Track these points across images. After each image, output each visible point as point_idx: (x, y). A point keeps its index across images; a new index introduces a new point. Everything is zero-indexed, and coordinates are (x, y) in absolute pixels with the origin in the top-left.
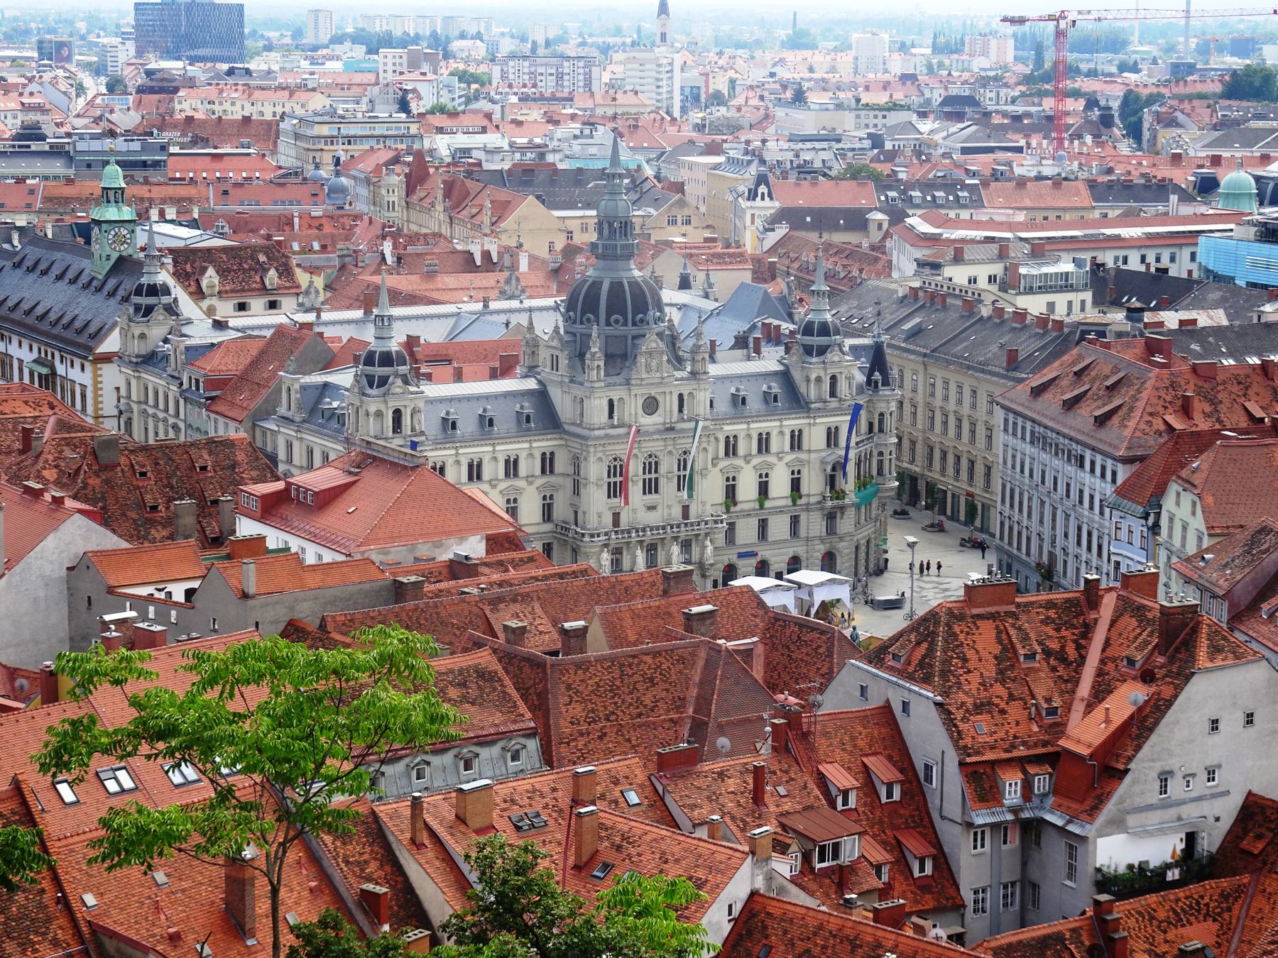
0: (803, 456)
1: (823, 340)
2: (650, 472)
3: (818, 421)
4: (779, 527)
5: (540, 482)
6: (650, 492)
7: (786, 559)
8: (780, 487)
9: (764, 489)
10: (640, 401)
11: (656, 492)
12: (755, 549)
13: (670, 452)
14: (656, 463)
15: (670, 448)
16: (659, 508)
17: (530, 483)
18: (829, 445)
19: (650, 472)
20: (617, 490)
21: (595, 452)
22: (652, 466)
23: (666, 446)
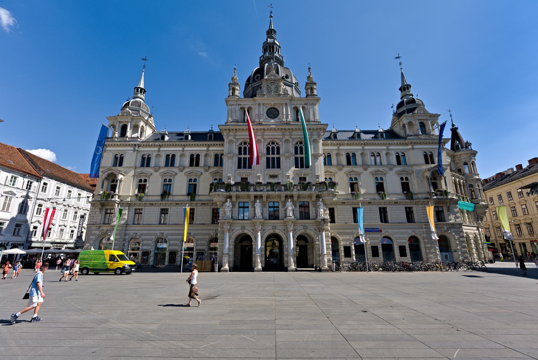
0: (407, 168)
1: (411, 106)
2: (273, 153)
3: (415, 147)
4: (396, 214)
5: (212, 170)
6: (273, 167)
7: (407, 236)
8: (393, 185)
9: (380, 187)
10: (265, 110)
11: (279, 167)
12: (380, 228)
13: (287, 141)
14: (278, 149)
15: (287, 137)
16: (280, 176)
17: (206, 171)
18: (427, 162)
19: (273, 153)
20: (245, 163)
21: (228, 136)
22: (273, 149)
23: (284, 135)
